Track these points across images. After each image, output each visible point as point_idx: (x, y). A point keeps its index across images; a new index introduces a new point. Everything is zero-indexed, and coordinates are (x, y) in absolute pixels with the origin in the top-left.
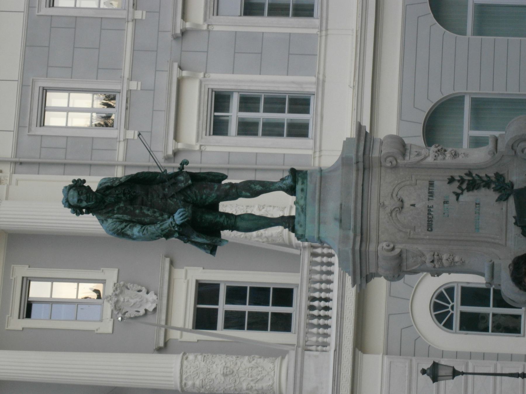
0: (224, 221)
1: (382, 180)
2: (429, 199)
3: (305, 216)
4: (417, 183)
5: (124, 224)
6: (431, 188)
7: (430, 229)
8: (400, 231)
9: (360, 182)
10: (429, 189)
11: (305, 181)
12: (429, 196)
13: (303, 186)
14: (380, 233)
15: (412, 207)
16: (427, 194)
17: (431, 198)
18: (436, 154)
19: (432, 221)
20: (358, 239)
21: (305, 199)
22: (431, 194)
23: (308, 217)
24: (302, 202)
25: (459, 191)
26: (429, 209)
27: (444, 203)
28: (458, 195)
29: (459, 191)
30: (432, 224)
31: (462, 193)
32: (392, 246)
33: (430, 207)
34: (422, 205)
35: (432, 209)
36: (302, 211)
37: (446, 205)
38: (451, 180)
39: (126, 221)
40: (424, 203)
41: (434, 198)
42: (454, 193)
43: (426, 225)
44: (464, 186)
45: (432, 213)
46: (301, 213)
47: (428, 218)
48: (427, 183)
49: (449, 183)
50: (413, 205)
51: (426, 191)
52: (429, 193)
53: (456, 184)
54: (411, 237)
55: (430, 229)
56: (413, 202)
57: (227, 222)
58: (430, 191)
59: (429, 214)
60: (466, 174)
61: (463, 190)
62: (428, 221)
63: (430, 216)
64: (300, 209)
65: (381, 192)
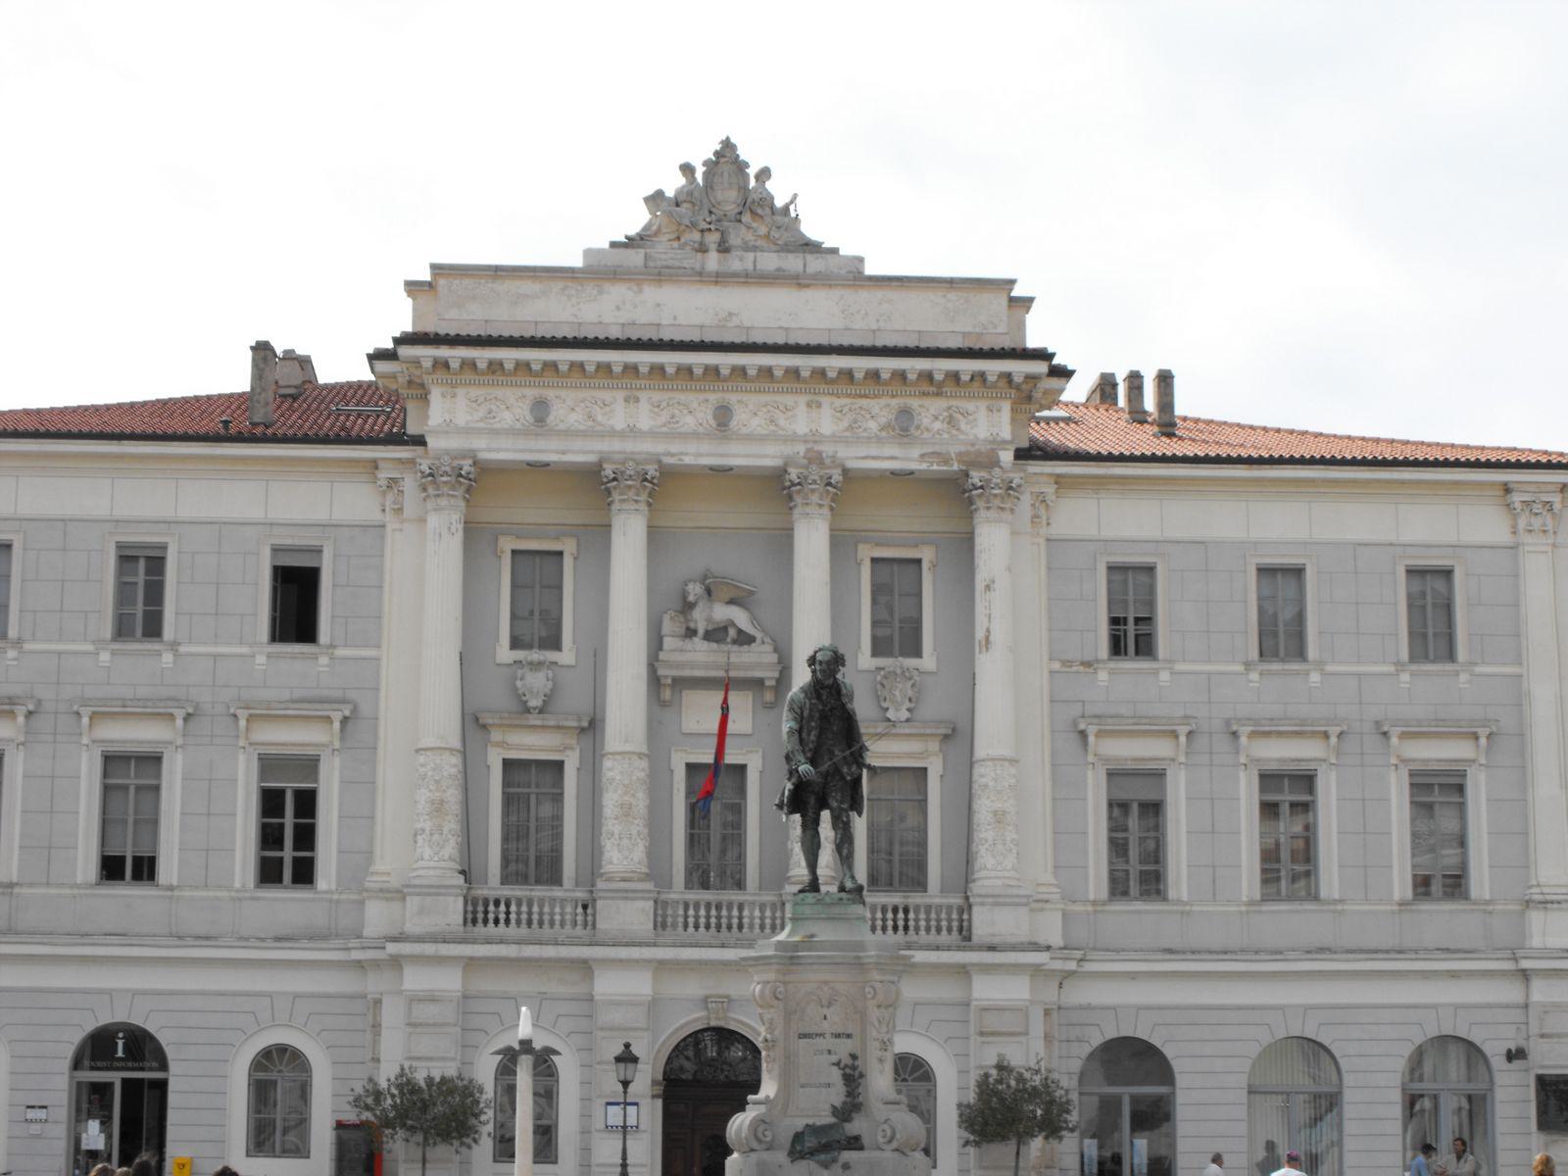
5: (799, 711)
22: (838, 1036)
25: (842, 1065)
28: (837, 1064)
29: (842, 1065)
31: (840, 1068)
32: (781, 997)
34: (826, 1027)
38: (854, 1057)
39: (802, 713)
44: (848, 1071)
48: (849, 1032)
50: (825, 1018)
53: (849, 1061)
56: (828, 1016)
59: (817, 1035)
61: (843, 1069)
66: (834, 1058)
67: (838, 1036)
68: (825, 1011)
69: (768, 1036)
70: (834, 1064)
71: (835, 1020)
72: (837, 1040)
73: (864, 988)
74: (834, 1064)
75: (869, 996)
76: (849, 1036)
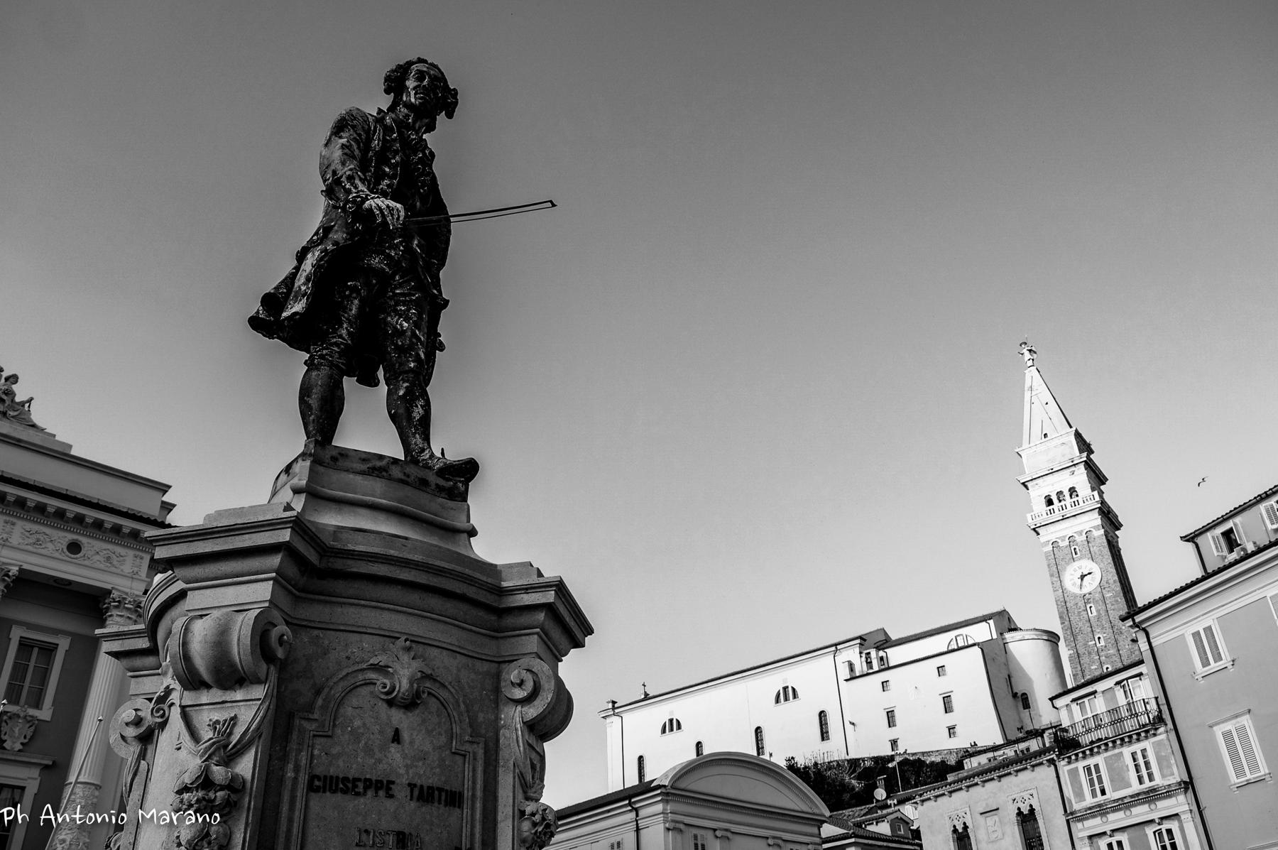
0: (341, 337)
1: (464, 660)
2: (412, 786)
3: (362, 473)
4: (458, 758)
7: (317, 783)
8: (318, 692)
10: (440, 790)
13: (433, 487)
14: (316, 632)
15: (390, 733)
17: (416, 793)
18: (537, 818)
19: (345, 792)
20: (312, 556)
22: (425, 795)
23: (359, 478)
24: (396, 472)
26: (383, 787)
30: (334, 792)
32: (280, 653)
33: (388, 789)
34: (395, 761)
35: (381, 793)
36: (374, 469)
40: (402, 771)
41: (413, 804)
45: (370, 793)
46: (370, 465)
47: (356, 780)
48: (455, 787)
50: (397, 738)
54: (297, 722)
55: (317, 783)
56: (405, 736)
57: (336, 344)
59: (368, 784)
62: (345, 779)
63: (361, 785)
64: (378, 464)
65: (435, 652)
68: (397, 717)
69: (219, 773)
71: (413, 751)
73: (497, 677)
76: (454, 799)
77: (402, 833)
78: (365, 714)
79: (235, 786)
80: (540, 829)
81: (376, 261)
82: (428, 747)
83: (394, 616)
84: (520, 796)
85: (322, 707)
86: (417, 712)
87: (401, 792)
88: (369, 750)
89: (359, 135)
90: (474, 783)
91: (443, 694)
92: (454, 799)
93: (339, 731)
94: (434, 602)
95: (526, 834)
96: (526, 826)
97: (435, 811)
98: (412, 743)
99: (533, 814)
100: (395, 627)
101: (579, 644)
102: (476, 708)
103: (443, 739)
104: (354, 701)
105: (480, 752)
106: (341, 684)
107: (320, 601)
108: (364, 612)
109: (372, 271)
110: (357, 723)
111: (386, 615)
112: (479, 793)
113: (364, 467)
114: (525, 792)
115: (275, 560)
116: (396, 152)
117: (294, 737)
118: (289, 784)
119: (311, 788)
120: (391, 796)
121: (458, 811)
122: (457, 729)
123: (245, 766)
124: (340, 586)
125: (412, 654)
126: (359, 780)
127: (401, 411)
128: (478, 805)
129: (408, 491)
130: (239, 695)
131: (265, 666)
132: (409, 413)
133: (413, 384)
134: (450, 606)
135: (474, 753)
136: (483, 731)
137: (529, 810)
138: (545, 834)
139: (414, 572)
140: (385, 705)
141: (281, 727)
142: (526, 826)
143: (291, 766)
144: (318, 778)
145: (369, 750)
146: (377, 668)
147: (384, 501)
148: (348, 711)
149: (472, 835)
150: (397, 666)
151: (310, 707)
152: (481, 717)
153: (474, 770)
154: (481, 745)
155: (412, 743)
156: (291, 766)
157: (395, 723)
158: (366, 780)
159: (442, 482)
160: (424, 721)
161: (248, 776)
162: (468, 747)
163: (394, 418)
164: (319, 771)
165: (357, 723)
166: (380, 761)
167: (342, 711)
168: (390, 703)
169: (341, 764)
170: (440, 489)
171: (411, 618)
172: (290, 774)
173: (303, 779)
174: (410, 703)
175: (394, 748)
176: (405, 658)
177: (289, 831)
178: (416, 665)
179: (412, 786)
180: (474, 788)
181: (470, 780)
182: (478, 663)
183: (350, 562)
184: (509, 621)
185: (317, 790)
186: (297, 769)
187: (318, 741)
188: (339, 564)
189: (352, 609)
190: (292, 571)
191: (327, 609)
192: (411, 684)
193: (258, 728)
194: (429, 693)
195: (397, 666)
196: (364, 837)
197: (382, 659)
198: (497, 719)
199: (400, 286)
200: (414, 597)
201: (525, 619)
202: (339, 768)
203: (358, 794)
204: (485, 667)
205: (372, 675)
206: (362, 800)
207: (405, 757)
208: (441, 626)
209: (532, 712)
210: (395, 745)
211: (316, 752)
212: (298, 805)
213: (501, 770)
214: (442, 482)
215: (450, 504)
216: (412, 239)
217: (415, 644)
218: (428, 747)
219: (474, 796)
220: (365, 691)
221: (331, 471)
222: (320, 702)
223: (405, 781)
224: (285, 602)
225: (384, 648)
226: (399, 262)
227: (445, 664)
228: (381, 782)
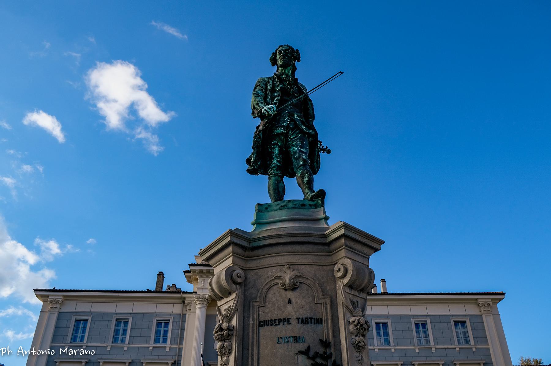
1: (317, 267)
2: (298, 319)
3: (278, 210)
4: (318, 305)
6: (313, 320)
7: (262, 323)
9: (311, 240)
10: (311, 318)
11: (313, 207)
12: (302, 318)
13: (308, 205)
14: (256, 271)
15: (287, 301)
16: (304, 317)
17: (300, 321)
19: (272, 325)
20: (245, 244)
21: (293, 208)
22: (305, 321)
23: (276, 212)
25: (311, 354)
26: (286, 321)
27: (294, 337)
28: (305, 353)
29: (311, 354)
30: (268, 325)
31: (309, 358)
32: (239, 280)
33: (288, 321)
34: (290, 311)
35: (286, 323)
36: (282, 207)
37: (291, 340)
38: (325, 344)
40: (293, 314)
41: (300, 325)
42: (309, 348)
43: (267, 319)
44: (318, 360)
45: (281, 324)
48: (318, 316)
49: (321, 341)
50: (290, 302)
51: (308, 316)
52: (307, 318)
53: (321, 350)
54: (251, 303)
55: (262, 323)
56: (293, 301)
58: (309, 320)
59: (280, 320)
60: (335, 361)
61: (313, 358)
62: (271, 320)
63: (277, 322)
65: (303, 267)
66: (302, 346)
67: (305, 321)
69: (225, 325)
70: (301, 352)
71: (299, 305)
72: (305, 326)
74: (301, 352)
75: (340, 274)
76: (318, 321)
77: (296, 337)
78: (277, 296)
79: (230, 329)
80: (358, 327)
81: (279, 130)
82: (304, 303)
83: (283, 257)
84: (349, 315)
85: (260, 296)
86: (297, 291)
87: (294, 322)
88: (279, 309)
89: (262, 87)
90: (327, 313)
91: (307, 282)
92: (318, 321)
93: (267, 304)
94: (297, 247)
95: (351, 330)
96: (351, 327)
97: (310, 327)
98: (296, 303)
99: (354, 322)
100: (284, 261)
101: (376, 250)
102: (325, 285)
103: (311, 299)
104: (271, 292)
105: (328, 301)
106: (266, 287)
107: (255, 259)
108: (271, 259)
109: (278, 135)
110: (274, 299)
111: (280, 258)
112: (329, 317)
113: (278, 207)
114: (352, 314)
115: (230, 249)
116: (278, 86)
117: (251, 309)
118: (251, 326)
119: (260, 326)
120: (290, 324)
121: (320, 325)
122: (316, 294)
123: (234, 322)
124: (259, 252)
125: (292, 270)
126: (276, 320)
127: (300, 182)
128: (330, 322)
129: (296, 210)
130: (230, 298)
131: (234, 286)
132: (303, 181)
133: (303, 170)
134: (304, 248)
135: (326, 302)
136: (330, 293)
137: (351, 320)
138: (362, 329)
139: (284, 238)
140: (284, 291)
141: (246, 306)
142: (351, 327)
143: (251, 319)
144: (262, 322)
145: (279, 309)
146: (277, 278)
147: (286, 217)
148: (270, 296)
149: (328, 334)
150: (285, 276)
151: (256, 298)
152: (328, 288)
153: (326, 308)
154: (329, 298)
155: (296, 303)
156: (251, 319)
157: (289, 297)
158: (279, 319)
159: (311, 203)
160: (301, 294)
161: (235, 325)
162: (323, 300)
163: (299, 185)
164: (262, 319)
165: (274, 299)
166: (284, 312)
167: (268, 296)
168: (285, 290)
169: (269, 315)
170: (311, 205)
171: (290, 256)
172: (251, 322)
173: (256, 323)
174: (294, 288)
175: (289, 306)
176: (288, 272)
177: (253, 342)
178: (293, 273)
179: (298, 319)
180: (327, 316)
181: (324, 312)
182: (325, 267)
183: (259, 242)
184: (333, 246)
185: (262, 326)
186: (253, 320)
187: (260, 309)
188: (256, 244)
189: (267, 259)
190: (240, 251)
191: (258, 261)
192: (290, 280)
193: (235, 308)
194: (300, 283)
195: (285, 276)
196: (280, 340)
197: (279, 274)
198: (336, 287)
199: (292, 135)
200: (289, 248)
201: (338, 244)
202: (269, 317)
203: (276, 325)
204: (329, 267)
205: (277, 281)
206: (278, 327)
207: (294, 308)
208: (303, 256)
209: (346, 280)
210: (289, 305)
211: (260, 313)
212: (255, 332)
213: (338, 307)
214: (311, 203)
215: (316, 210)
216: (293, 115)
217: (290, 265)
218: (304, 303)
219: (327, 319)
220: (275, 287)
221: (265, 213)
222: (259, 295)
223: (295, 317)
224: (241, 263)
225: (277, 269)
226: (288, 126)
227: (306, 271)
228: (285, 319)
